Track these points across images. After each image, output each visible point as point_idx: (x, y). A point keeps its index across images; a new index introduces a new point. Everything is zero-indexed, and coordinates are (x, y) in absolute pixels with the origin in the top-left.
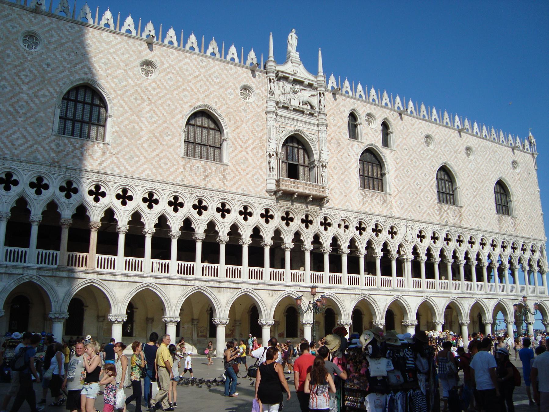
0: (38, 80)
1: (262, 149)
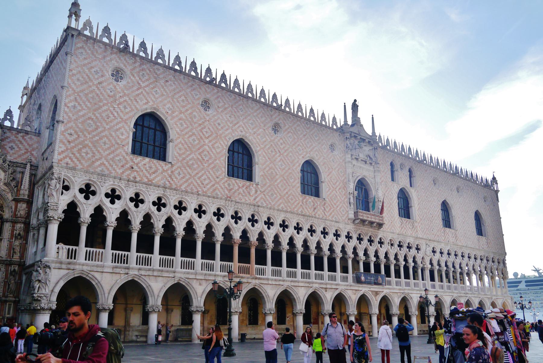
0: (214, 135)
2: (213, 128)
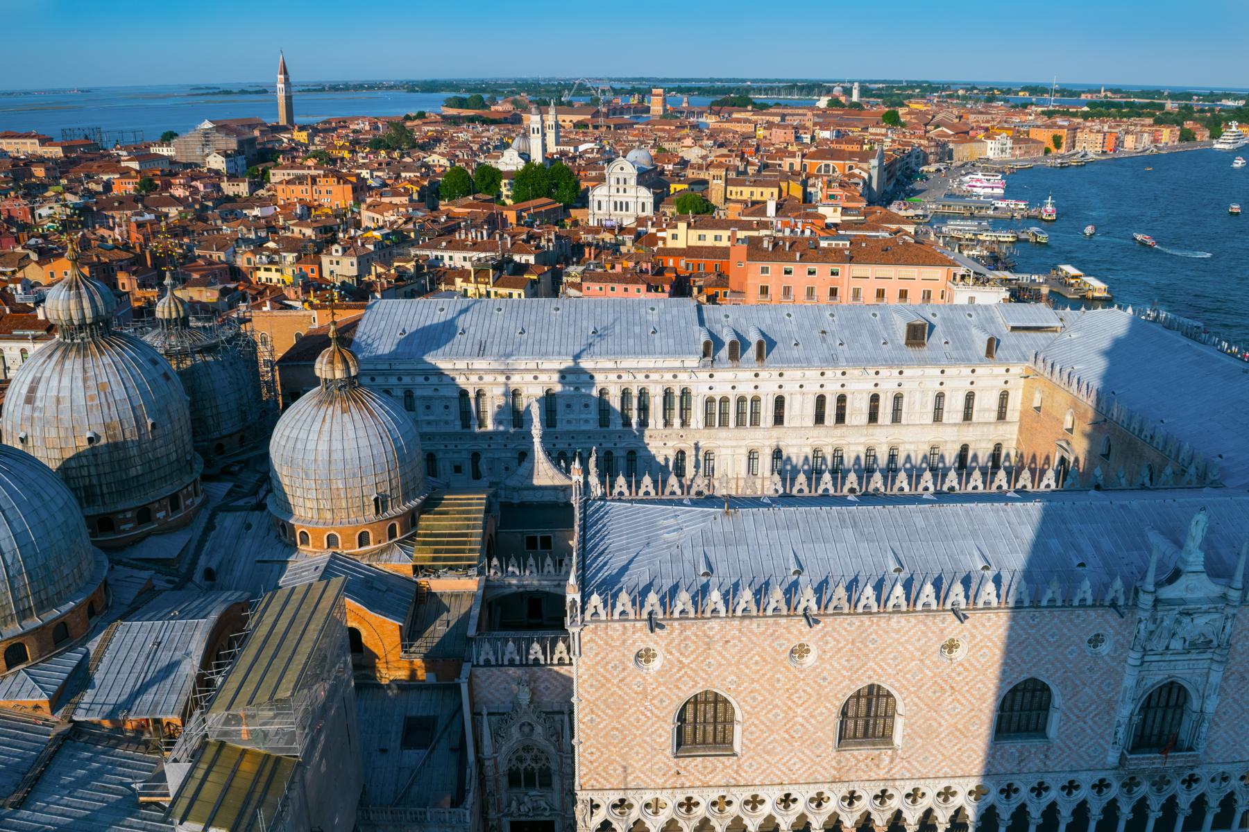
0: (812, 700)
1: (1108, 713)
2: (812, 688)
